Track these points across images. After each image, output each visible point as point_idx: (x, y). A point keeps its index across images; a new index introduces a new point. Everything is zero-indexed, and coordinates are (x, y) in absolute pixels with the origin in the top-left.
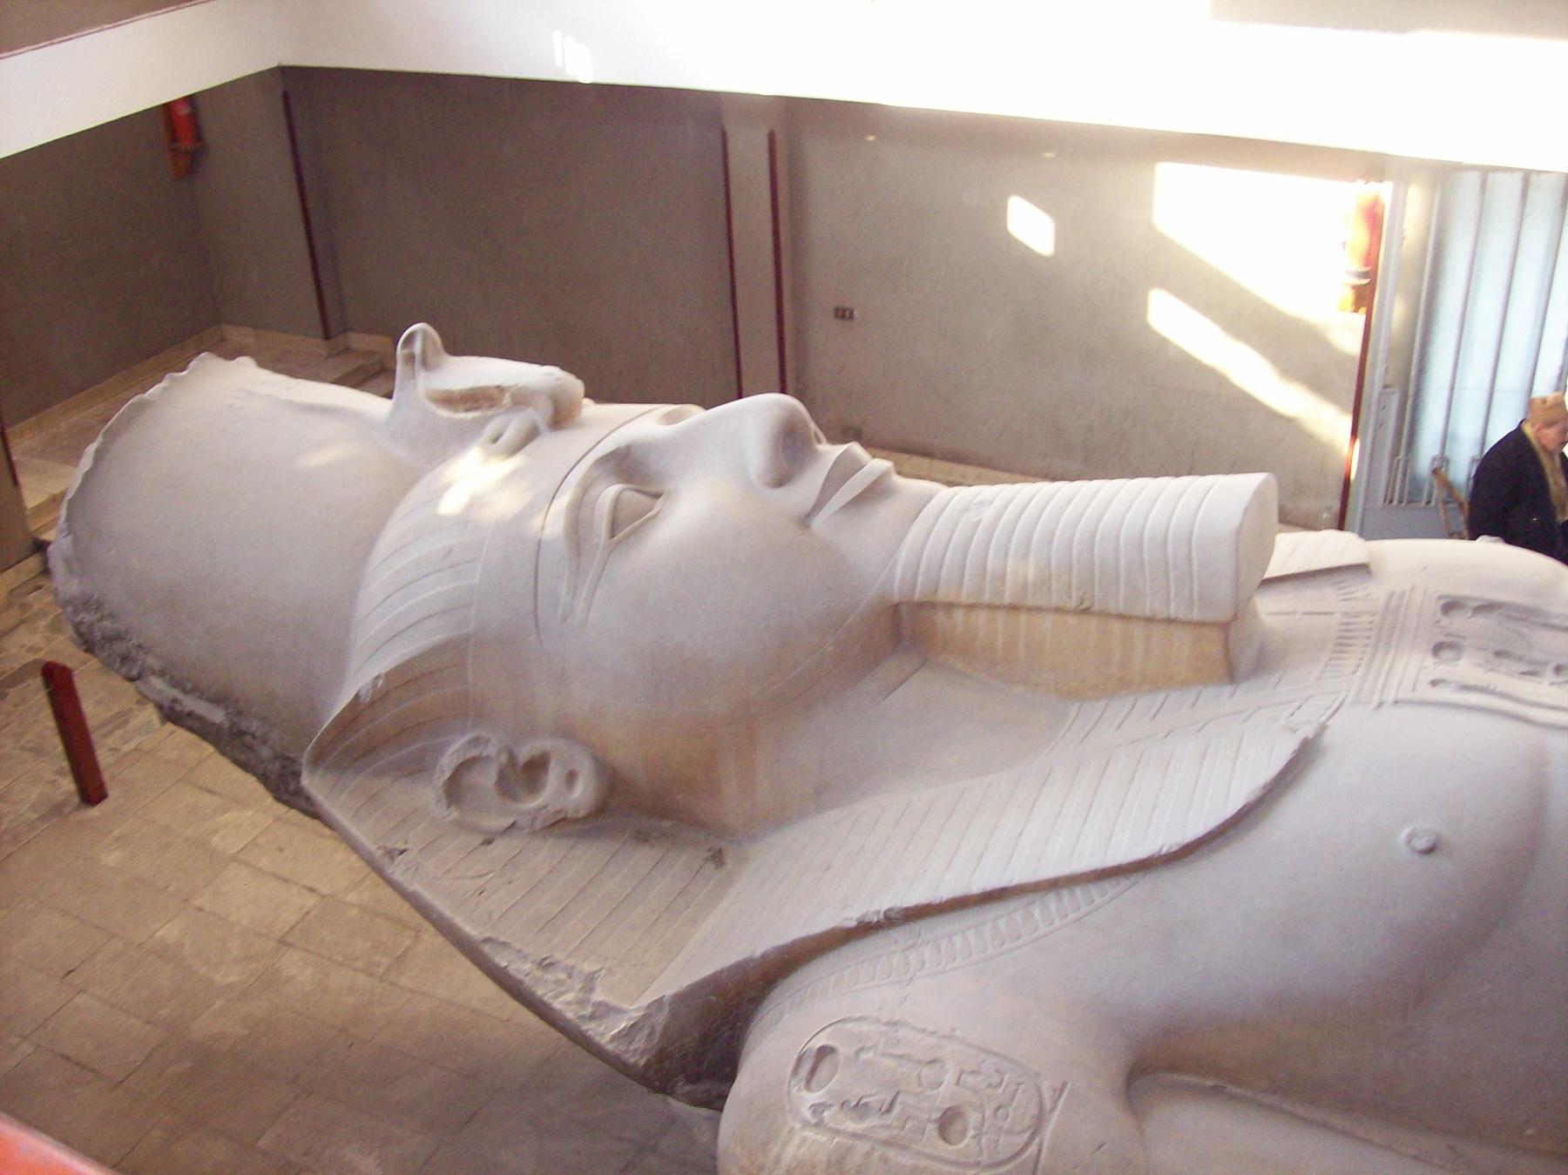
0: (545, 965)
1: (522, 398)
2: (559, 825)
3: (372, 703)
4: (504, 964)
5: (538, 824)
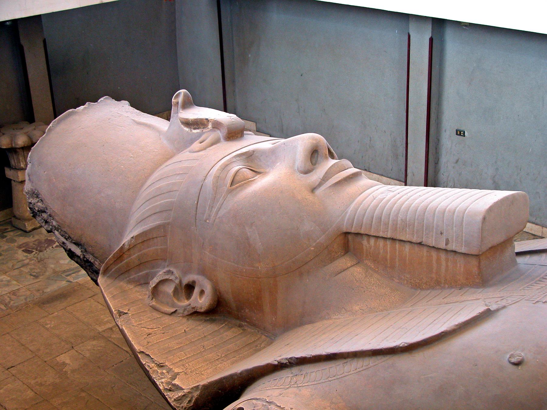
0: (161, 366)
2: (195, 314)
3: (129, 249)
4: (144, 363)
5: (186, 313)
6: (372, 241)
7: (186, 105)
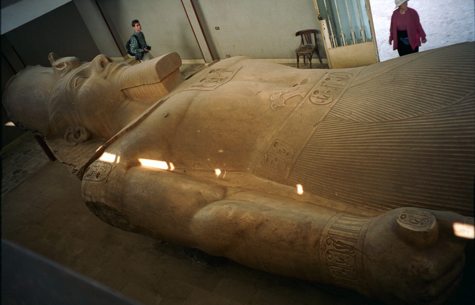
0: (70, 165)
1: (67, 63)
6: (131, 89)
7: (56, 59)
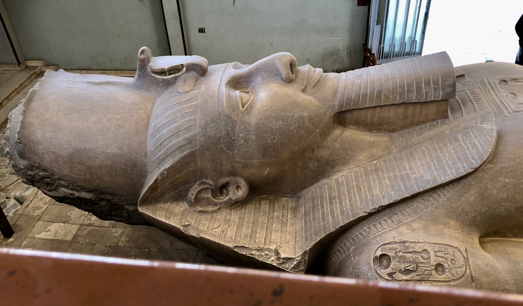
0: (259, 250)
4: (244, 253)
